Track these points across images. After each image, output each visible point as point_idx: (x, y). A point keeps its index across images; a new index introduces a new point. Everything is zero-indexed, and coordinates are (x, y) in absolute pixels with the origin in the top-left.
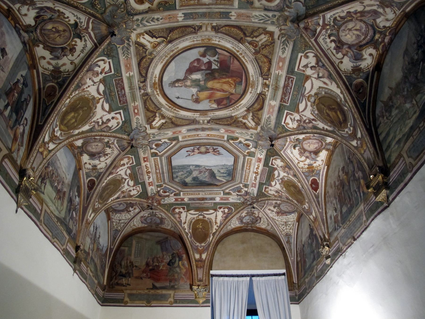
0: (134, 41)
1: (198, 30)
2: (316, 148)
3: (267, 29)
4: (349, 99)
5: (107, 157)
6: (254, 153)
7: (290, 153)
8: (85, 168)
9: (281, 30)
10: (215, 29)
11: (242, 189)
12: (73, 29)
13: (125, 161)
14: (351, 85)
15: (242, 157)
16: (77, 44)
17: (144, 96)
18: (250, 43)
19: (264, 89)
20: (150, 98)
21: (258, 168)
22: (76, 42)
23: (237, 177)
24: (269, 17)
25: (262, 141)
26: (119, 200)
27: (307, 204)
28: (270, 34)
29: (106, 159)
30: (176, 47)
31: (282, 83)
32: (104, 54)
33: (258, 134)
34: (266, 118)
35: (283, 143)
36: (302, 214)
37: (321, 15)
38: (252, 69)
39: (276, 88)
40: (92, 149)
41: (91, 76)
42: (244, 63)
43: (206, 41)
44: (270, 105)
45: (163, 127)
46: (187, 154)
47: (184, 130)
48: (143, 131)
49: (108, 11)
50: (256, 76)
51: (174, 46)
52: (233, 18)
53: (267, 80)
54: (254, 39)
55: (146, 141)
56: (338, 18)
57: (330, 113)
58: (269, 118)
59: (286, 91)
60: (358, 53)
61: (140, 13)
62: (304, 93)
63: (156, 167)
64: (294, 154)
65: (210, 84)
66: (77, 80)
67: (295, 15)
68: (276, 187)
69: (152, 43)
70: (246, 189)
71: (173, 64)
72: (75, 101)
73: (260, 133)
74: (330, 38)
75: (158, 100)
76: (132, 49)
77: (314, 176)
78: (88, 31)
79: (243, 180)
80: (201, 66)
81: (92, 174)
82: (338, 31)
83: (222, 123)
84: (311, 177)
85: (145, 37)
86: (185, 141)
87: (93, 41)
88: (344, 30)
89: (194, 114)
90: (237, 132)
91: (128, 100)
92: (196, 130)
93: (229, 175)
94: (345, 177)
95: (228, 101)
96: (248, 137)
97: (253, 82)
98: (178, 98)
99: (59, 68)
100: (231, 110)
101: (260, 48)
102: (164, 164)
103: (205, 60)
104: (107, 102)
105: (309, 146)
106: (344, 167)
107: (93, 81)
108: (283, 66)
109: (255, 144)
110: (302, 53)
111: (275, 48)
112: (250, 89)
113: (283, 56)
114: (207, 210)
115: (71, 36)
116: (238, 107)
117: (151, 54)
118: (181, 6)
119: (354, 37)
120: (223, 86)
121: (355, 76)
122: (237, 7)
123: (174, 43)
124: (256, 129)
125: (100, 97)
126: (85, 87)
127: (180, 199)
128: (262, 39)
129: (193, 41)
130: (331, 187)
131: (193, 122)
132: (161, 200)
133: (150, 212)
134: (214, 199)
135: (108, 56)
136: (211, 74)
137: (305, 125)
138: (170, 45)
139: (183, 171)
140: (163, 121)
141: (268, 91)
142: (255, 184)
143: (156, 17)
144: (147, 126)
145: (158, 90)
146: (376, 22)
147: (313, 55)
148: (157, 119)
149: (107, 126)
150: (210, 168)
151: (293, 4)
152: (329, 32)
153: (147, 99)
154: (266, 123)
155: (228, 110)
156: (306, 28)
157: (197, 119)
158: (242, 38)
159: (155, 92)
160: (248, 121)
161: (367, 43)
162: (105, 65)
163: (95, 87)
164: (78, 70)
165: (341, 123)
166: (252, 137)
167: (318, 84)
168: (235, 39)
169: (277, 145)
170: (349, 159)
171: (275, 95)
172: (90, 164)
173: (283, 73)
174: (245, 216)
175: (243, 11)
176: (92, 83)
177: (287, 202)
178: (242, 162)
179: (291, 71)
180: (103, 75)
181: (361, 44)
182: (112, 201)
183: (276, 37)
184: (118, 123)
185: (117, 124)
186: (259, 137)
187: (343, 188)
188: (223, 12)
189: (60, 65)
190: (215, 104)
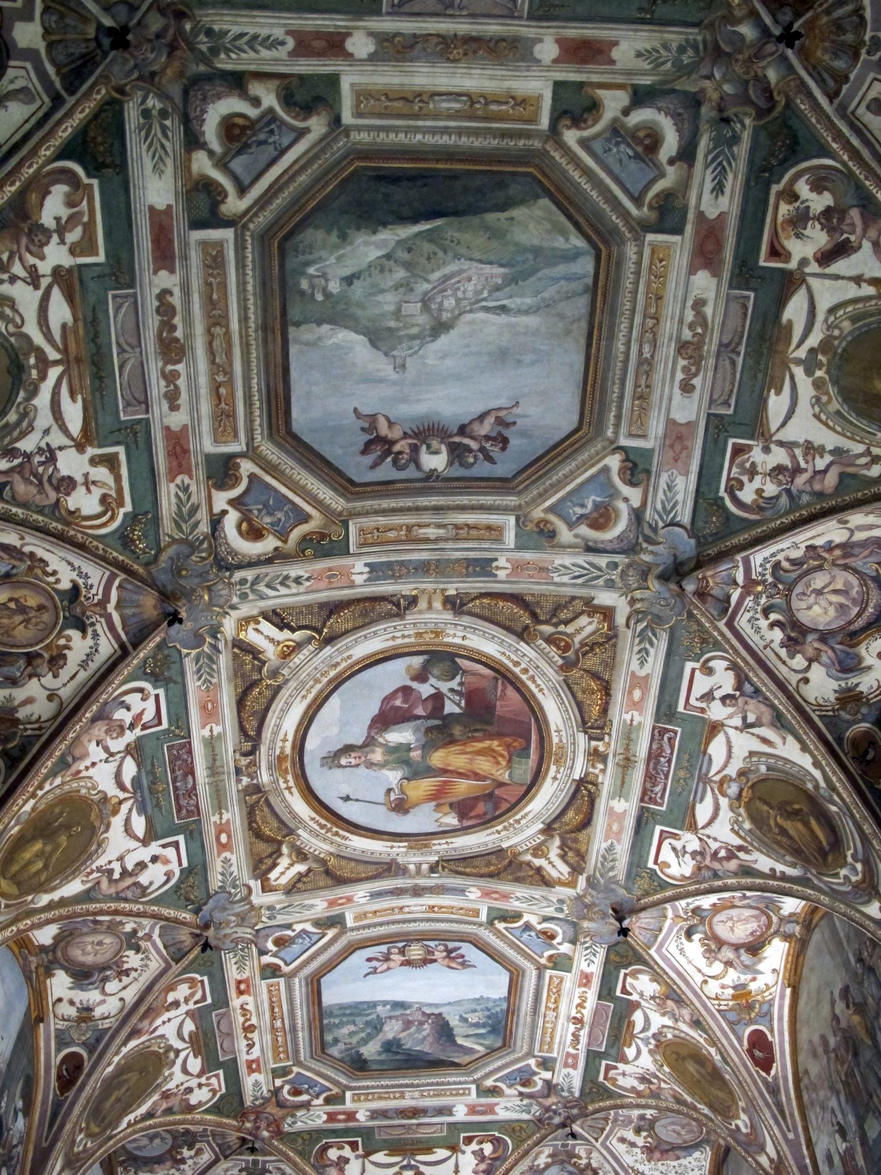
0: (229, 638)
1: (406, 609)
2: (752, 934)
3: (595, 602)
4: (840, 780)
5: (126, 980)
6: (570, 958)
7: (676, 953)
9: (633, 602)
10: (453, 604)
11: (535, 1074)
12: (66, 603)
14: (839, 740)
15: (534, 973)
16: (71, 644)
17: (250, 795)
18: (550, 640)
19: (593, 767)
20: (267, 800)
21: (581, 1006)
22: (69, 639)
23: (520, 1035)
24: (599, 569)
25: (591, 920)
26: (151, 1122)
27: (743, 1116)
28: (604, 614)
29: (124, 988)
30: (345, 655)
31: (642, 748)
32: (145, 673)
33: (579, 898)
34: (602, 851)
35: (653, 923)
36: (728, 1150)
37: (739, 557)
38: (556, 712)
39: (627, 763)
42: (534, 696)
43: (428, 637)
44: (611, 812)
45: (300, 885)
46: (367, 967)
47: (362, 894)
48: (242, 900)
49: (164, 557)
50: (570, 732)
51: (341, 653)
52: (502, 574)
53: (602, 739)
54: (562, 628)
56: (785, 565)
57: (788, 825)
58: (610, 849)
59: (655, 768)
60: (848, 654)
61: (251, 564)
62: (708, 771)
63: (272, 1009)
64: (686, 956)
65: (438, 758)
66: (63, 746)
67: (670, 560)
68: (639, 1062)
69: (279, 643)
70: (547, 1075)
71: (334, 701)
72: (51, 806)
73: (584, 896)
74: (767, 618)
75: (288, 806)
76: (224, 661)
77: (756, 1023)
78: (105, 609)
79: (537, 1046)
80: (413, 706)
81: (75, 1036)
82: (788, 598)
84: (747, 1025)
85: (259, 627)
86: (364, 927)
87: (117, 637)
88: (804, 594)
91: (202, 807)
92: (398, 892)
93: (494, 1030)
94: (856, 1019)
95: (490, 805)
96: (550, 911)
97: (561, 747)
98: (347, 799)
99: (15, 710)
100: (499, 832)
101: (576, 653)
102: (298, 1001)
103: (425, 690)
105: (732, 929)
106: (845, 992)
107: (106, 749)
108: (642, 699)
109: (570, 932)
110: (693, 660)
111: (619, 650)
112: (553, 768)
113: (642, 673)
114: (428, 1150)
115: (56, 624)
116: (518, 821)
117: (275, 673)
119: (832, 612)
120: (476, 762)
121: (848, 717)
122: (512, 546)
123: (341, 644)
124: (572, 884)
125: (122, 795)
126: (82, 767)
127: (344, 1113)
128: (582, 629)
129: (394, 638)
130: (815, 1055)
131: (389, 870)
132: (283, 1118)
133: (247, 1162)
134: (446, 1110)
135: (156, 678)
136: (441, 730)
137: (716, 865)
138: (328, 650)
139: (354, 1023)
140: (301, 868)
141: (603, 771)
142: (575, 1057)
143: (293, 574)
144: (252, 883)
145: (290, 777)
147: (725, 664)
148: (284, 862)
149: (137, 884)
150: (436, 1011)
151: (661, 532)
152: (763, 600)
153: (256, 801)
156: (702, 594)
157: (400, 860)
158: (527, 627)
159: (281, 781)
161: (869, 626)
162: (144, 705)
163: (112, 767)
164: (67, 715)
165: (824, 854)
166: (561, 910)
167: (745, 744)
169: (637, 932)
170: (860, 960)
171: (623, 783)
172: (72, 1003)
173: (646, 719)
174: (548, 1166)
175: (528, 556)
176: (104, 756)
177: (678, 1112)
179: (666, 711)
180: (138, 732)
181: (852, 628)
182: (129, 1125)
183: (620, 619)
184: (169, 875)
185: (165, 878)
186: (584, 907)
187: (856, 1054)
188: (476, 560)
189: (16, 703)
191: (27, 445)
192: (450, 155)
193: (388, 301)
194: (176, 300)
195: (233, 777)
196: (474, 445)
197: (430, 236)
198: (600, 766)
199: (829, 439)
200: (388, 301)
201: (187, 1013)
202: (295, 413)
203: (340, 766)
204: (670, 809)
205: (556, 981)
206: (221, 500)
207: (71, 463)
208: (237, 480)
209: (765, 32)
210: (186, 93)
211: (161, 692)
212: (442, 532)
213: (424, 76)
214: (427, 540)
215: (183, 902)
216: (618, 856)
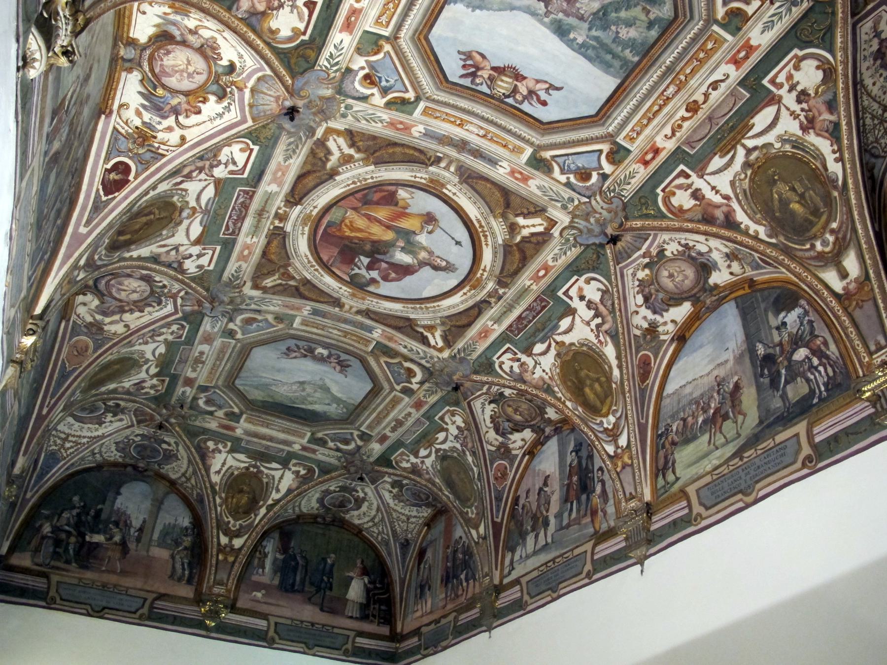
2: (168, 53)
5: (691, 244)
7: (246, 57)
8: (744, 273)
13: (683, 200)
15: (402, 34)
18: (293, 278)
19: (285, 212)
25: (321, 98)
26: (844, 127)
29: (698, 242)
34: (295, 157)
38: (301, 245)
39: (260, 213)
40: (686, 277)
41: (529, 373)
42: (312, 255)
45: (533, 210)
48: (574, 228)
52: (308, 308)
54: (284, 282)
55: (593, 202)
56: (155, 304)
59: (241, 212)
61: (419, 364)
62: (203, 218)
65: (389, 236)
71: (425, 294)
72: (568, 389)
76: (460, 345)
80: (386, 269)
83: (407, 151)
86: (522, 139)
89: (454, 194)
90: (380, 125)
92: (477, 153)
95: (369, 197)
96: (358, 106)
97: (306, 225)
98: (458, 243)
100: (372, 178)
102: (634, 102)
103: (374, 274)
104: (557, 326)
107: (535, 367)
109: (347, 86)
112: (314, 213)
116: (354, 183)
117: (443, 324)
118: (369, 341)
123: (404, 315)
124: (329, 131)
125: (553, 344)
126: (547, 377)
131: (469, 177)
135: (491, 365)
138: (412, 316)
139: (616, 39)
140: (521, 221)
141: (279, 208)
145: (479, 275)
146: (99, 300)
148: (525, 232)
149: (601, 300)
154: (297, 147)
155: (379, 179)
157: (456, 180)
158: (304, 285)
159: (484, 277)
160: (340, 150)
163: (541, 359)
168: (314, 286)
171: (266, 202)
172: (729, 266)
173: (243, 239)
178: (412, 14)
180: (519, 355)
184: (588, 282)
185: (592, 282)
186: (324, 110)
190: (399, 197)
191: (458, 446)
192: (279, 417)
193: (318, 395)
194: (389, 428)
195: (505, 298)
196: (302, 351)
197: (294, 403)
198: (280, 211)
199: (137, 348)
200: (318, 395)
201: (702, 177)
202: (369, 388)
203: (448, 262)
204: (234, 189)
205: (384, 19)
206: (415, 387)
207: (453, 431)
208: (404, 387)
209: (167, 421)
210: (355, 454)
211: (495, 358)
212: (331, 330)
213: (282, 436)
214: (339, 330)
215: (602, 259)
216: (283, 153)
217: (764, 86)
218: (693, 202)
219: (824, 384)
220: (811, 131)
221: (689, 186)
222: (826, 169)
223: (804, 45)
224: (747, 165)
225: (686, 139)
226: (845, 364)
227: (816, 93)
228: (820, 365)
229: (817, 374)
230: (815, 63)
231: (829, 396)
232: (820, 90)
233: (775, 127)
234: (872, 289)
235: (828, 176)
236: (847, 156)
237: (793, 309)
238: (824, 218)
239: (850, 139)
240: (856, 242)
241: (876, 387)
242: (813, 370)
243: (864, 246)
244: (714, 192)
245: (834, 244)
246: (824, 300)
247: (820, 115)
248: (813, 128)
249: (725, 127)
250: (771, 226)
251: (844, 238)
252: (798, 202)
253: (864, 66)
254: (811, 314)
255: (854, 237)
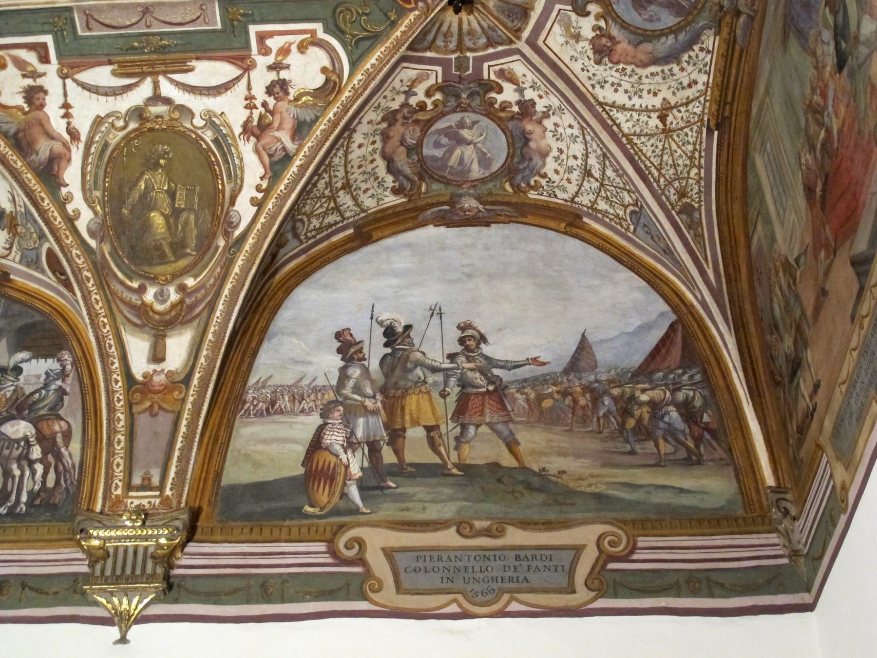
26: (294, 168)
81: (31, 245)
182: (259, 204)
201: (64, 77)
217: (247, 33)
218: (20, 101)
219: (30, 493)
220: (253, 139)
221: (35, 75)
222: (233, 202)
223: (334, 29)
224: (138, 113)
225: (90, 8)
226: (79, 481)
227: (297, 99)
228: (41, 461)
229: (27, 473)
230: (327, 63)
231: (27, 514)
232: (304, 99)
233: (214, 96)
234: (183, 401)
235: (228, 213)
236: (270, 206)
237: (46, 357)
238: (183, 263)
239: (290, 188)
240: (202, 325)
241: (110, 539)
242: (25, 463)
243: (210, 336)
244: (63, 111)
245: (173, 306)
246: (107, 373)
247: (278, 129)
248: (258, 138)
249: (155, 40)
250: (104, 220)
251: (192, 307)
252: (166, 217)
253: (371, 115)
254: (69, 380)
255: (205, 315)
